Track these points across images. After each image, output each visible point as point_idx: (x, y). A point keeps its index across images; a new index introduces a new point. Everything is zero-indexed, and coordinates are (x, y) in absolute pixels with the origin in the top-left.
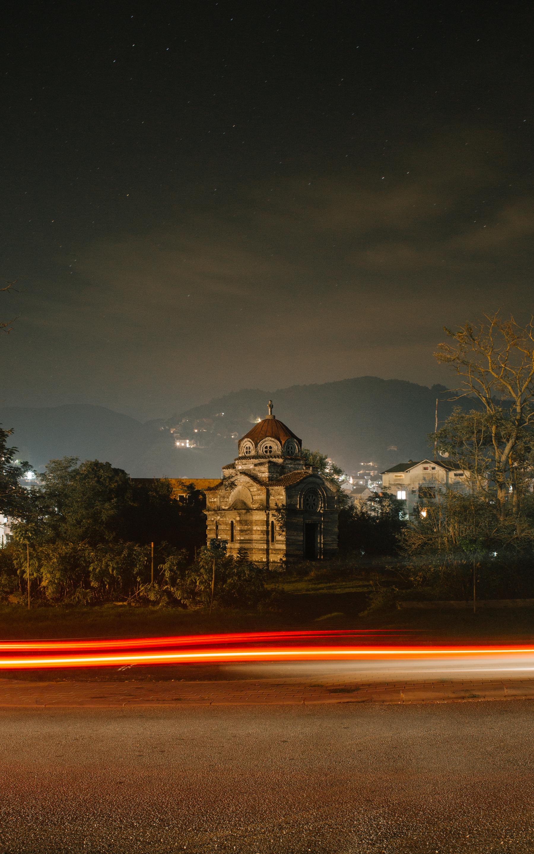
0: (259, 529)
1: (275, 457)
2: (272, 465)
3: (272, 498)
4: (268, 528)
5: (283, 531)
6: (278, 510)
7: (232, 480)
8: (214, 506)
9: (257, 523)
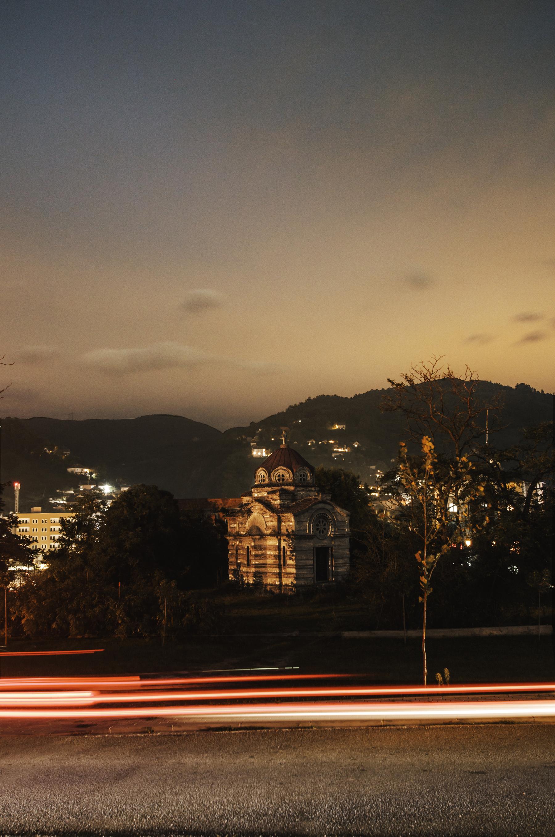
0: (272, 553)
1: (287, 485)
2: (283, 494)
3: (283, 524)
4: (280, 553)
5: (293, 555)
6: (288, 535)
7: (249, 507)
8: (234, 532)
9: (270, 548)
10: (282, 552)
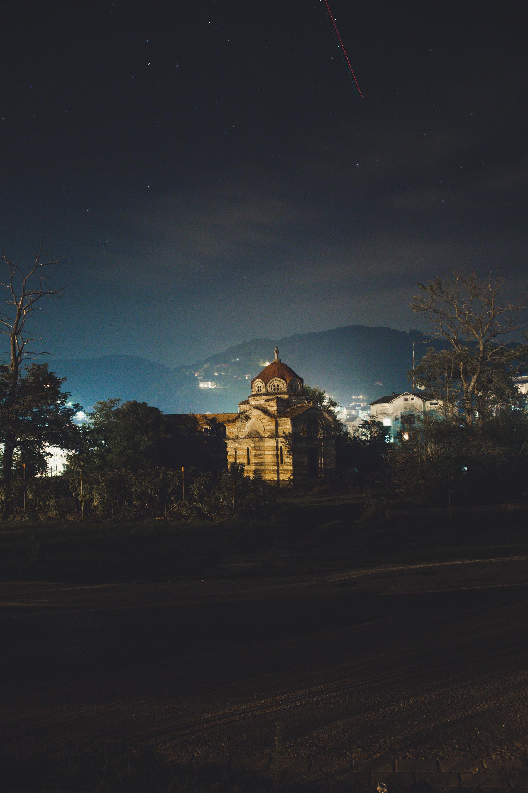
0: (270, 453)
1: (282, 394)
2: (280, 401)
3: (280, 427)
4: (277, 452)
5: (290, 455)
6: (285, 437)
7: (247, 414)
8: (232, 436)
9: (268, 448)
10: (279, 452)
